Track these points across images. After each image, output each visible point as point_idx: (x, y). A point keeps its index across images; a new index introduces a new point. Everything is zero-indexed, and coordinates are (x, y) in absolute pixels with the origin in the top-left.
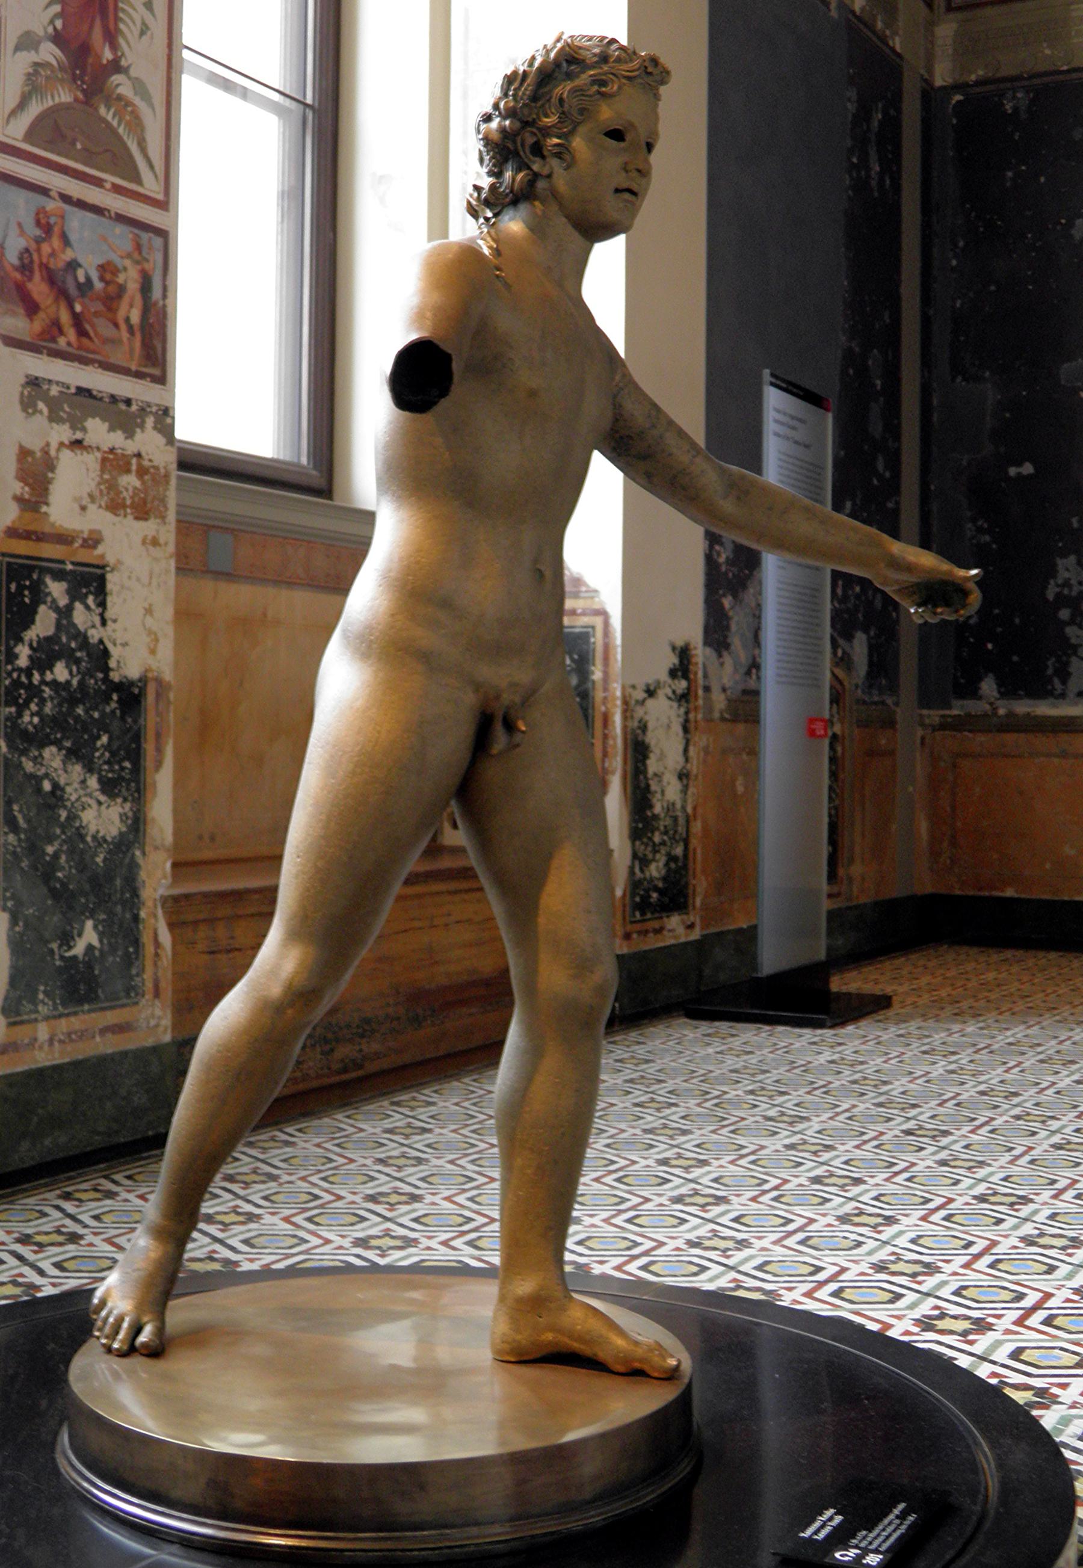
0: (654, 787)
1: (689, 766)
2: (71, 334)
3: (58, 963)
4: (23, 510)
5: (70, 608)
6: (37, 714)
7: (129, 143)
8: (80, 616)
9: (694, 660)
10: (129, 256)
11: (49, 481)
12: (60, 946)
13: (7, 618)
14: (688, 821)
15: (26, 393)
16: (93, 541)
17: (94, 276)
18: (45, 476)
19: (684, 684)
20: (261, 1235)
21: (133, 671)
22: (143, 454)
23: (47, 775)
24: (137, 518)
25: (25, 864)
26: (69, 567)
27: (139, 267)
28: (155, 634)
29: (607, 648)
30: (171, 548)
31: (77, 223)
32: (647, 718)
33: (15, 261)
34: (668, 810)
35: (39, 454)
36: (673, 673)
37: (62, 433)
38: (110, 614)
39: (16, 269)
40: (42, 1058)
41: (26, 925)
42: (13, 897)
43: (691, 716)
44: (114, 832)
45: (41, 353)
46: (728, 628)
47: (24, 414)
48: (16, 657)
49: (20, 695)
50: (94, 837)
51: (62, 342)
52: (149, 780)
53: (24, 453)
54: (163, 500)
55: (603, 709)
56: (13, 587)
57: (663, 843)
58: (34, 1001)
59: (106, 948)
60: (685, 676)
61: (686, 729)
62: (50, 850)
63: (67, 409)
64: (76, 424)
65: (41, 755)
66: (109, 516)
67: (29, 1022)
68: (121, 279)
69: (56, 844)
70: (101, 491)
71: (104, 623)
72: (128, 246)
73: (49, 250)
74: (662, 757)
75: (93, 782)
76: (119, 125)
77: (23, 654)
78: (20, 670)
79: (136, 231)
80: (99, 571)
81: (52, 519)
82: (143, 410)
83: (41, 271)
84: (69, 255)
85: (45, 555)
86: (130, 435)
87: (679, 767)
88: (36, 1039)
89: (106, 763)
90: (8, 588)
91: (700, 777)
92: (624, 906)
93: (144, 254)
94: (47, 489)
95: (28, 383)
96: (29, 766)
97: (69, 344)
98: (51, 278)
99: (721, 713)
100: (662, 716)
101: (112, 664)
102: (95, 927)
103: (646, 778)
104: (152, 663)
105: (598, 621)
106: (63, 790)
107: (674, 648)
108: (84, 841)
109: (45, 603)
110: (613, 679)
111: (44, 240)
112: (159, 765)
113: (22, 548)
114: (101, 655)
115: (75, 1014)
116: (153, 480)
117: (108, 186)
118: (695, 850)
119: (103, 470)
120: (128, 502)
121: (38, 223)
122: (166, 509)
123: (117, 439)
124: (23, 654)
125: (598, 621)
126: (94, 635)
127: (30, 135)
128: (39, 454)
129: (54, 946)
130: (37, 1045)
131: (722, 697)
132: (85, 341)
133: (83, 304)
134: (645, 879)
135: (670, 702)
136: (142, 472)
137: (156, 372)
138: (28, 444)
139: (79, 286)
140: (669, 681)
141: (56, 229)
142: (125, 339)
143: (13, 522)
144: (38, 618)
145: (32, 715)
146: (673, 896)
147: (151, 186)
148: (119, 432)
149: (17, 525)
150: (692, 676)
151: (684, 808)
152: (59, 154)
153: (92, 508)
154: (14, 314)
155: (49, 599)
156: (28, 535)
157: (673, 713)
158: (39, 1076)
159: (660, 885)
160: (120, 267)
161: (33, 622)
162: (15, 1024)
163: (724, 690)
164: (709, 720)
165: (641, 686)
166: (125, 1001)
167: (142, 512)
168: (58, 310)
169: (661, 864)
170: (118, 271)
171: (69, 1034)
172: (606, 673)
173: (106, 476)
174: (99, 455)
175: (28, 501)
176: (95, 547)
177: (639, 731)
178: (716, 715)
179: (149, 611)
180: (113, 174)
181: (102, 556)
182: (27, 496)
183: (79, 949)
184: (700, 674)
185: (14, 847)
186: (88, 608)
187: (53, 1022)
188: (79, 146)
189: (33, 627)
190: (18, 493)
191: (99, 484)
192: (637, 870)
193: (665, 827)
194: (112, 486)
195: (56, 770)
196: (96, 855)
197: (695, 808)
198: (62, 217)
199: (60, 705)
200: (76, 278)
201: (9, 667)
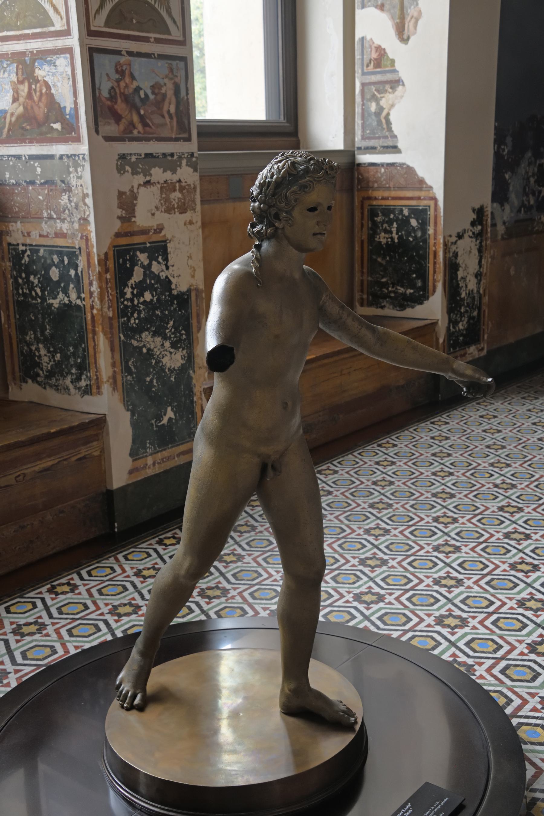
0: (461, 284)
1: (481, 270)
2: (140, 127)
4: (122, 223)
5: (150, 265)
6: (137, 318)
7: (162, 12)
8: (155, 268)
9: (485, 214)
10: (167, 76)
11: (135, 205)
12: (155, 422)
14: (480, 298)
16: (160, 229)
17: (149, 92)
18: (133, 203)
19: (479, 227)
20: (242, 570)
21: (183, 288)
22: (182, 180)
23: (144, 346)
24: (180, 213)
26: (148, 245)
27: (172, 82)
28: (194, 267)
29: (436, 217)
30: (199, 224)
31: (138, 66)
32: (457, 250)
33: (107, 95)
34: (469, 294)
35: (128, 193)
36: (473, 224)
37: (141, 179)
38: (169, 264)
39: (107, 99)
40: (150, 472)
43: (484, 244)
44: (179, 365)
45: (125, 141)
46: (508, 189)
48: (125, 294)
50: (169, 369)
51: (135, 132)
52: (194, 337)
53: (121, 194)
54: (194, 201)
55: (434, 249)
56: (121, 261)
57: (466, 311)
58: (145, 448)
59: (178, 418)
60: (481, 224)
61: (480, 251)
62: (148, 379)
63: (141, 166)
64: (146, 173)
65: (141, 337)
66: (167, 215)
67: (143, 457)
68: (163, 91)
69: (151, 376)
70: (161, 204)
71: (167, 268)
72: (166, 71)
73: (124, 85)
74: (466, 267)
75: (167, 344)
76: (155, 3)
77: (128, 291)
78: (127, 300)
79: (169, 62)
80: (163, 244)
81: (138, 224)
82: (180, 158)
83: (121, 97)
84: (135, 84)
85: (135, 242)
86: (174, 171)
87: (476, 271)
88: (147, 465)
89: (172, 334)
90: (119, 262)
91: (488, 274)
92: (444, 346)
93: (175, 71)
94: (134, 210)
95: (119, 158)
96: (135, 343)
97: (139, 132)
98: (126, 99)
99: (502, 236)
100: (467, 249)
101: (173, 286)
102: (172, 410)
103: (457, 281)
104: (193, 282)
105: (432, 203)
106: (153, 350)
107: (474, 210)
108: (165, 372)
109: (137, 265)
110: (437, 235)
111: (121, 80)
113: (123, 241)
115: (165, 450)
116: (188, 192)
117: (152, 40)
118: (484, 311)
119: (161, 194)
120: (176, 206)
121: (117, 71)
122: (196, 205)
123: (168, 175)
125: (432, 203)
126: (163, 275)
127: (107, 23)
128: (128, 193)
129: (153, 422)
131: (503, 227)
132: (147, 129)
133: (145, 111)
134: (456, 331)
135: (470, 239)
136: (182, 189)
137: (186, 135)
138: (122, 189)
139: (142, 100)
140: (471, 228)
141: (127, 72)
142: (168, 122)
144: (134, 273)
145: (135, 320)
146: (472, 336)
147: (176, 34)
148: (169, 172)
150: (484, 223)
151: (478, 291)
152: (124, 29)
153: (158, 213)
154: (109, 124)
155: (140, 263)
156: (127, 234)
157: (473, 245)
158: (148, 480)
159: (465, 332)
160: (163, 84)
161: (132, 275)
162: (136, 460)
163: (504, 223)
164: (494, 239)
165: (454, 234)
166: (188, 440)
167: (183, 210)
168: (132, 115)
169: (465, 322)
170: (162, 86)
171: (162, 459)
172: (435, 231)
173: (164, 196)
174: (159, 186)
175: (125, 217)
176: (160, 232)
177: (453, 258)
178: (499, 237)
179: (190, 257)
180: (154, 32)
181: (165, 236)
183: (165, 421)
184: (489, 220)
186: (159, 263)
187: (154, 455)
188: (134, 21)
190: (120, 215)
191: (160, 200)
192: (451, 328)
193: (467, 303)
194: (167, 200)
195: (148, 342)
196: (170, 377)
197: (484, 291)
198: (130, 65)
199: (148, 312)
200: (140, 96)
201: (122, 300)
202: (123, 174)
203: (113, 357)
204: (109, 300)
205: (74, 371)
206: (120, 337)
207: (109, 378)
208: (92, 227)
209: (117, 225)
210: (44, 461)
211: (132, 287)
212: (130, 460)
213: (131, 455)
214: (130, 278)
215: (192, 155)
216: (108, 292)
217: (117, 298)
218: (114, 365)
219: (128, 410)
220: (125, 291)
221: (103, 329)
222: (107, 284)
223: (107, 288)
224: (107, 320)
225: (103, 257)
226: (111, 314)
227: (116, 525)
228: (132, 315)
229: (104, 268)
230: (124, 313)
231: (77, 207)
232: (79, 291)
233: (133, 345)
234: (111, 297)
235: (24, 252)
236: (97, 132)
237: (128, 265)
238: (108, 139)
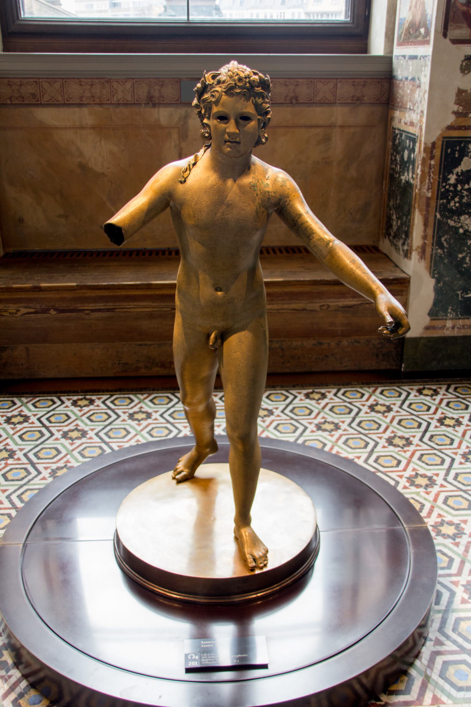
3: (460, 299)
4: (457, 117)
6: (458, 202)
12: (462, 293)
13: (444, 164)
15: (464, 64)
25: (446, 261)
40: (447, 333)
41: (444, 283)
42: (438, 273)
47: (462, 74)
48: (449, 179)
49: (450, 195)
53: (460, 92)
56: (449, 151)
58: (446, 312)
62: (460, 256)
65: (459, 219)
69: (464, 254)
77: (452, 179)
78: (450, 185)
88: (445, 326)
95: (465, 60)
96: (451, 223)
109: (468, 156)
115: (468, 318)
124: (452, 179)
129: (459, 293)
130: (445, 328)
138: (463, 87)
143: (452, 123)
144: (462, 163)
145: (455, 203)
149: (453, 124)
154: (460, 28)
156: (460, 128)
158: (445, 340)
161: (460, 164)
175: (462, 113)
182: (460, 111)
185: (440, 254)
187: (455, 321)
189: (459, 167)
195: (467, 225)
201: (444, 184)
202: (466, 74)
203: (425, 231)
204: (430, 182)
205: (403, 236)
206: (436, 216)
207: (418, 247)
208: (424, 120)
209: (451, 119)
210: (348, 300)
211: (457, 174)
212: (428, 318)
213: (429, 314)
214: (456, 166)
216: (430, 176)
217: (439, 182)
218: (425, 237)
219: (433, 277)
220: (449, 177)
221: (419, 206)
222: (430, 168)
223: (429, 173)
224: (424, 200)
225: (430, 145)
226: (429, 195)
227: (403, 365)
228: (453, 198)
229: (429, 155)
230: (444, 194)
231: (421, 102)
232: (413, 173)
233: (449, 225)
234: (432, 181)
235: (397, 134)
236: (445, 35)
237: (457, 155)
238: (455, 42)
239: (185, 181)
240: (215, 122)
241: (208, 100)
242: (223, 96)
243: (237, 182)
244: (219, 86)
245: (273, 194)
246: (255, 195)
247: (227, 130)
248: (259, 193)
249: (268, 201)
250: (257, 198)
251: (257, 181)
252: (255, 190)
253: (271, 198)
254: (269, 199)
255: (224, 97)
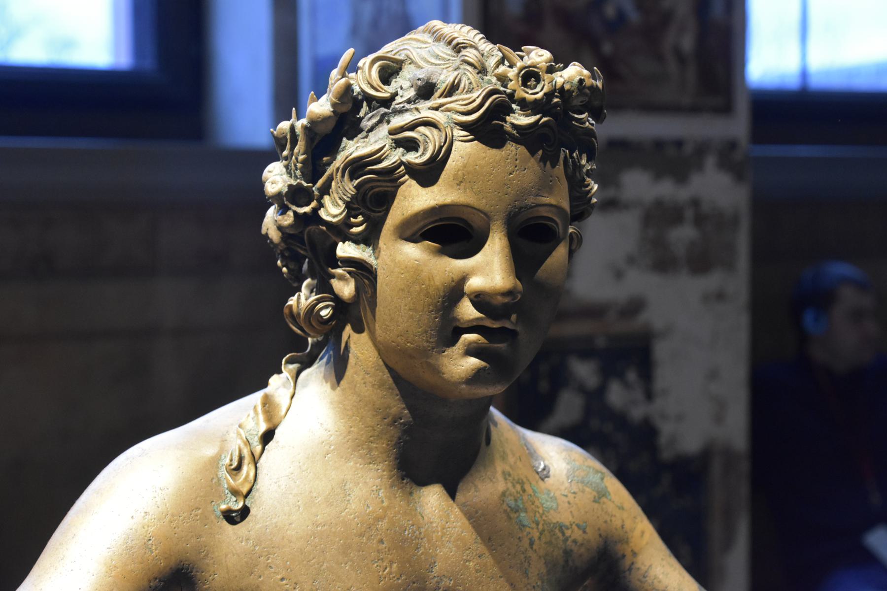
5: (601, 391)
8: (616, 395)
16: (635, 307)
71: (649, 395)
82: (702, 149)
101: (663, 440)
112: (728, 544)
114: (646, 434)
123: (666, 189)
136: (700, 220)
179: (713, 375)
186: (627, 385)
215: (732, 145)
239: (245, 512)
240: (413, 252)
241: (379, 161)
242: (457, 145)
243: (459, 496)
244: (429, 103)
245: (577, 534)
246: (526, 543)
247: (475, 283)
248: (536, 534)
249: (567, 562)
250: (534, 557)
251: (518, 487)
252: (522, 526)
253: (575, 548)
254: (567, 553)
255: (465, 151)
